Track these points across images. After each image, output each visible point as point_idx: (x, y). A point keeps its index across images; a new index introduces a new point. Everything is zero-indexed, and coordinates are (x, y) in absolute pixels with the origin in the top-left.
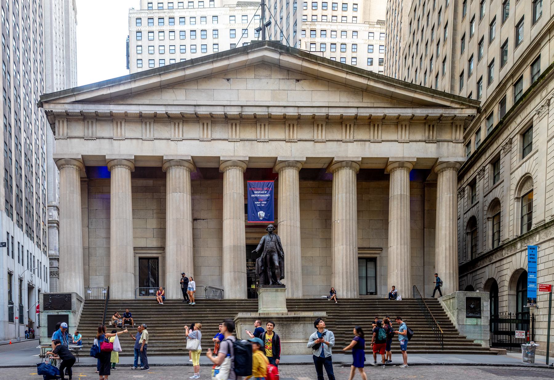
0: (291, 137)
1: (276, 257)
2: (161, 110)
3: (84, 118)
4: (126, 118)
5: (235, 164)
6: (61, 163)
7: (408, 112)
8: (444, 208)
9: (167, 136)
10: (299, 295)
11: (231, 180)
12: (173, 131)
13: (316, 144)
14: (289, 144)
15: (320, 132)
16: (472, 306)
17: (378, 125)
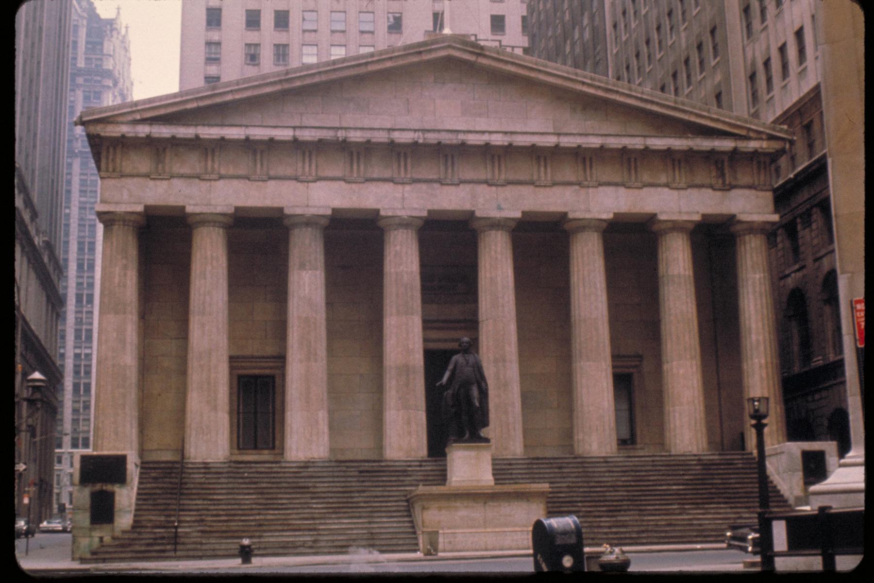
0: (497, 176)
1: (475, 392)
2: (284, 134)
3: (153, 145)
4: (222, 143)
5: (405, 224)
6: (108, 219)
7: (679, 143)
8: (751, 296)
9: (289, 172)
10: (516, 448)
11: (398, 248)
12: (300, 165)
13: (538, 189)
14: (494, 188)
15: (542, 169)
16: (812, 466)
17: (635, 159)
